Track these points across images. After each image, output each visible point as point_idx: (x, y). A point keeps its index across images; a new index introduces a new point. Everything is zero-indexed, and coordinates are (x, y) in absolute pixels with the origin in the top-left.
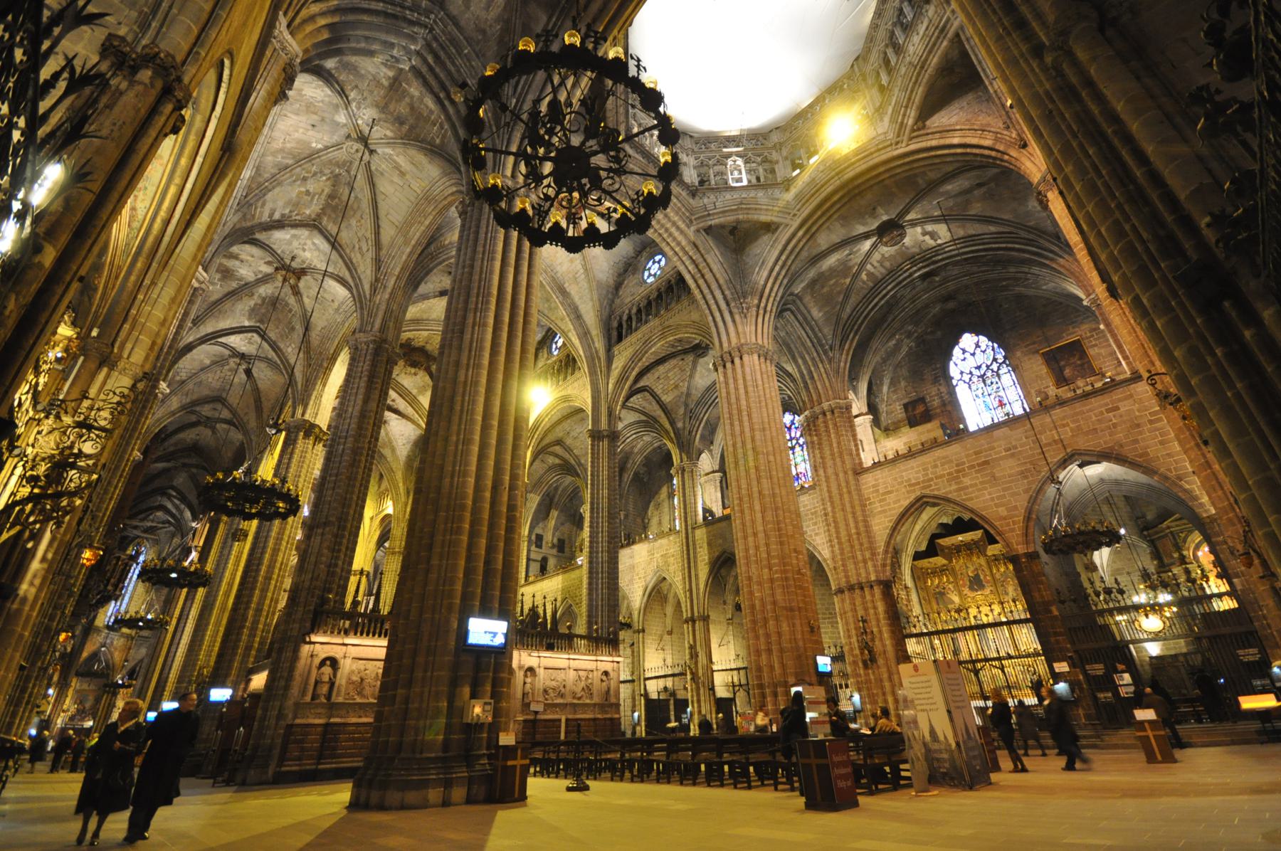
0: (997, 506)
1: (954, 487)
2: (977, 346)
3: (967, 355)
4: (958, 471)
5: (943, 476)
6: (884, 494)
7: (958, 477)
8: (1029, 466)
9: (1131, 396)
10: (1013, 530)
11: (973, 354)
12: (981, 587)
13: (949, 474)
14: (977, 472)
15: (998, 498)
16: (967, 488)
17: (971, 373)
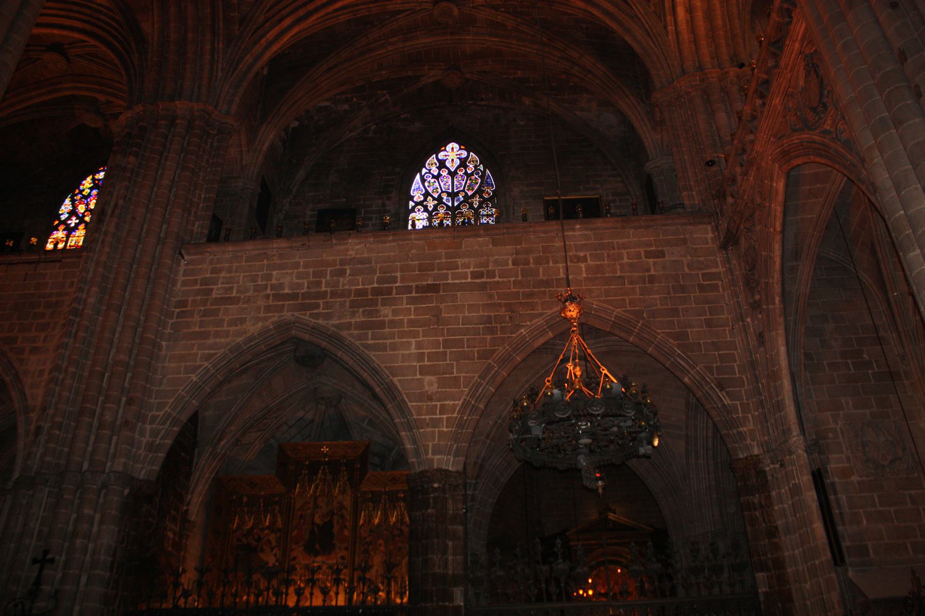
0: (424, 371)
1: (359, 318)
2: (463, 163)
3: (444, 173)
4: (377, 292)
5: (344, 294)
6: (217, 301)
7: (373, 303)
8: (502, 311)
9: (684, 242)
10: (436, 423)
11: (453, 174)
12: (327, 548)
13: (360, 293)
14: (412, 301)
15: (431, 357)
16: (382, 325)
17: (440, 199)
